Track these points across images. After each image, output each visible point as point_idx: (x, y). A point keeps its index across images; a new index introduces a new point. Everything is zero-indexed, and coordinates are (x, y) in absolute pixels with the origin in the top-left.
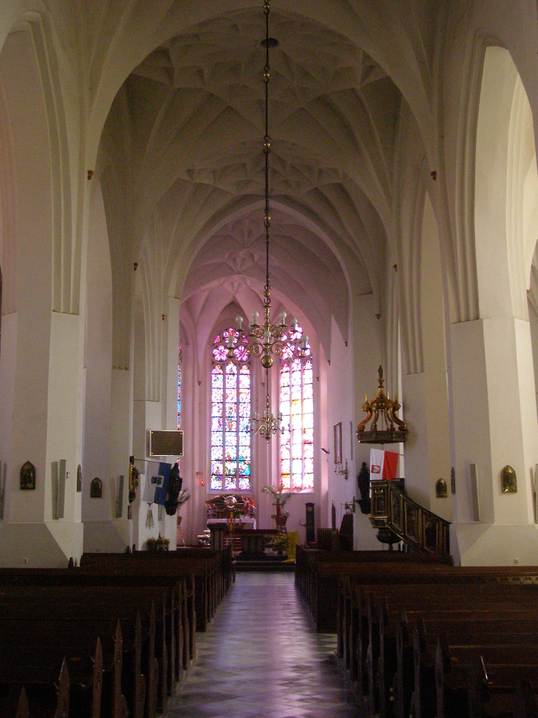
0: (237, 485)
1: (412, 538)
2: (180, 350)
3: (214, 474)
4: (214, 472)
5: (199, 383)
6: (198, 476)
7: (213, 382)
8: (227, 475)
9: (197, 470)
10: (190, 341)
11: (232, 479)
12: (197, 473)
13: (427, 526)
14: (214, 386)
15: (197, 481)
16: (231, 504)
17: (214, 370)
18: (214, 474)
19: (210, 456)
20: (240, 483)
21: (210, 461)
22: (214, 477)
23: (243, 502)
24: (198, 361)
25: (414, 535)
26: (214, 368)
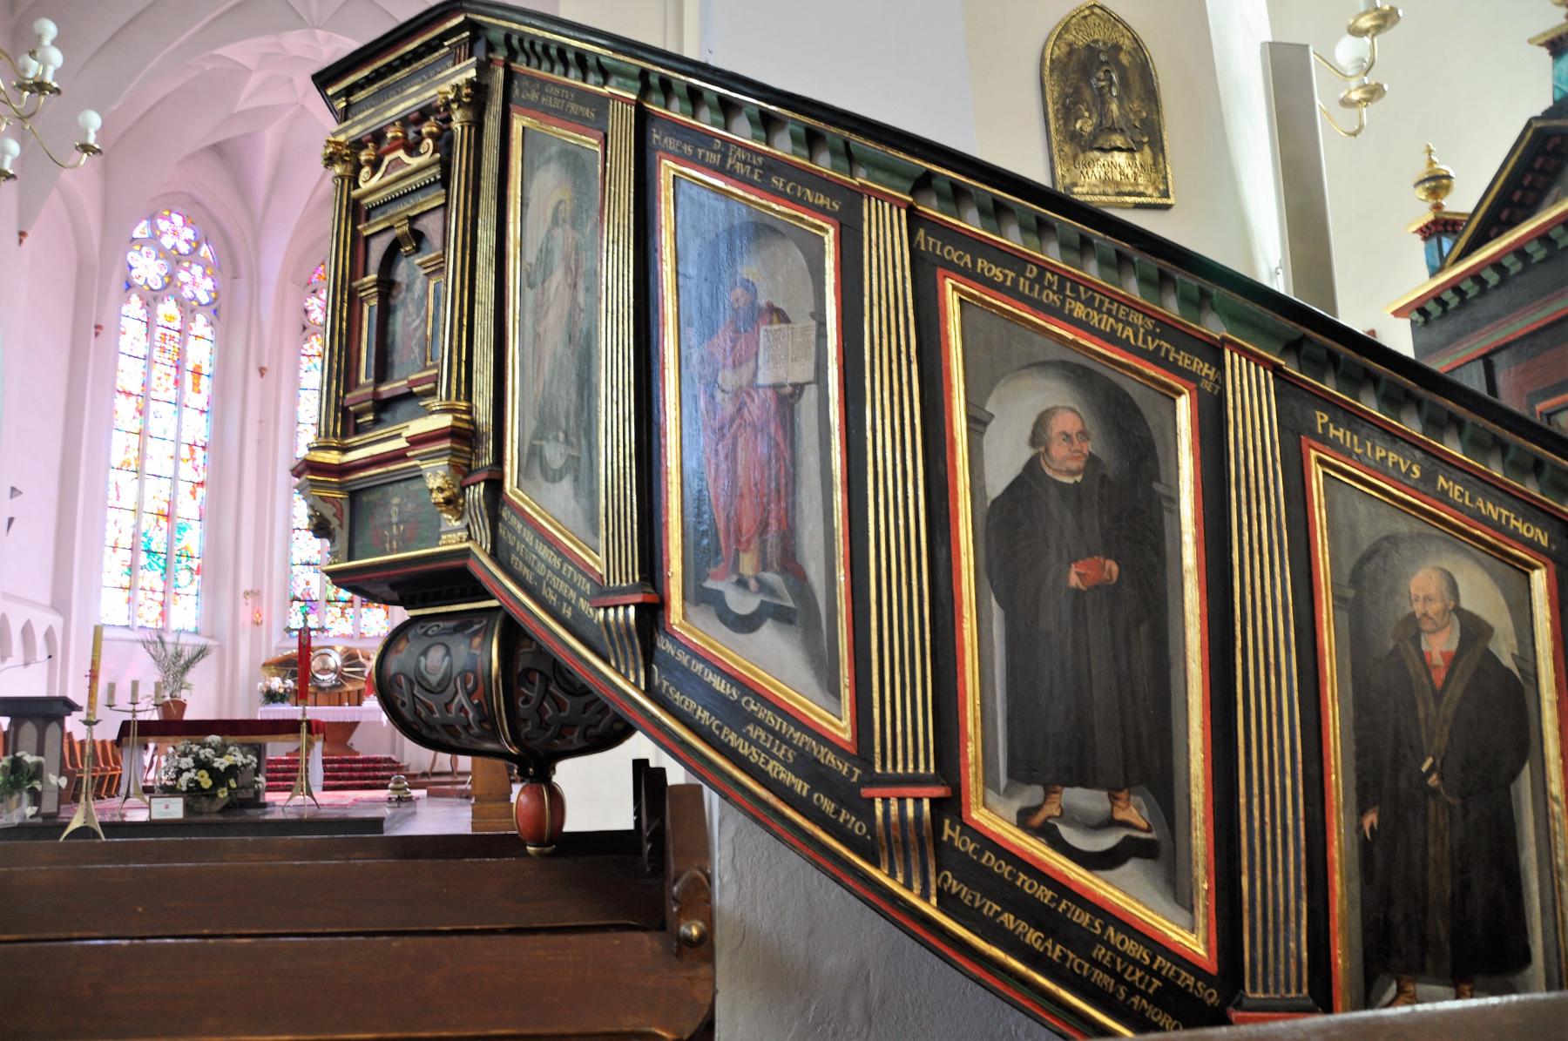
0: (356, 625)
1: (775, 664)
2: (216, 292)
3: (296, 599)
4: (298, 595)
5: (262, 371)
6: (250, 600)
7: (302, 374)
8: (328, 601)
9: (246, 584)
10: (244, 270)
11: (343, 609)
12: (247, 593)
13: (1006, 460)
14: (304, 384)
15: (245, 614)
16: (325, 671)
17: (306, 346)
18: (296, 599)
19: (288, 553)
20: (363, 621)
21: (288, 565)
22: (296, 603)
23: (362, 666)
24: (259, 316)
25: (793, 612)
26: (307, 340)
